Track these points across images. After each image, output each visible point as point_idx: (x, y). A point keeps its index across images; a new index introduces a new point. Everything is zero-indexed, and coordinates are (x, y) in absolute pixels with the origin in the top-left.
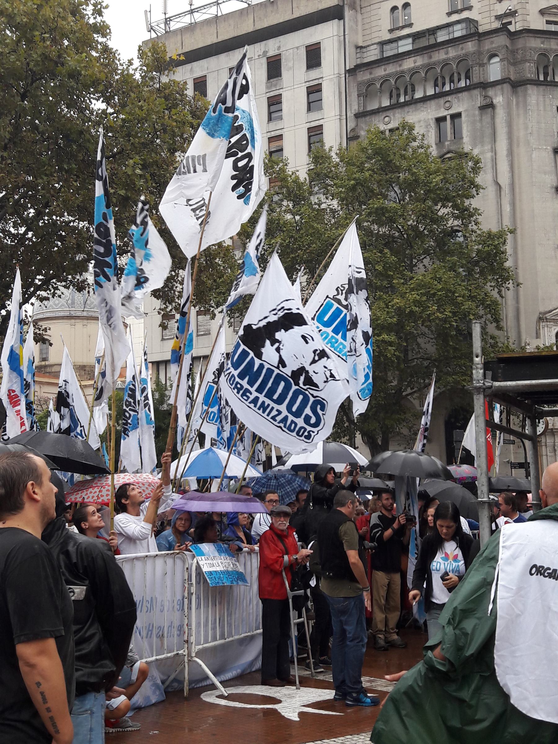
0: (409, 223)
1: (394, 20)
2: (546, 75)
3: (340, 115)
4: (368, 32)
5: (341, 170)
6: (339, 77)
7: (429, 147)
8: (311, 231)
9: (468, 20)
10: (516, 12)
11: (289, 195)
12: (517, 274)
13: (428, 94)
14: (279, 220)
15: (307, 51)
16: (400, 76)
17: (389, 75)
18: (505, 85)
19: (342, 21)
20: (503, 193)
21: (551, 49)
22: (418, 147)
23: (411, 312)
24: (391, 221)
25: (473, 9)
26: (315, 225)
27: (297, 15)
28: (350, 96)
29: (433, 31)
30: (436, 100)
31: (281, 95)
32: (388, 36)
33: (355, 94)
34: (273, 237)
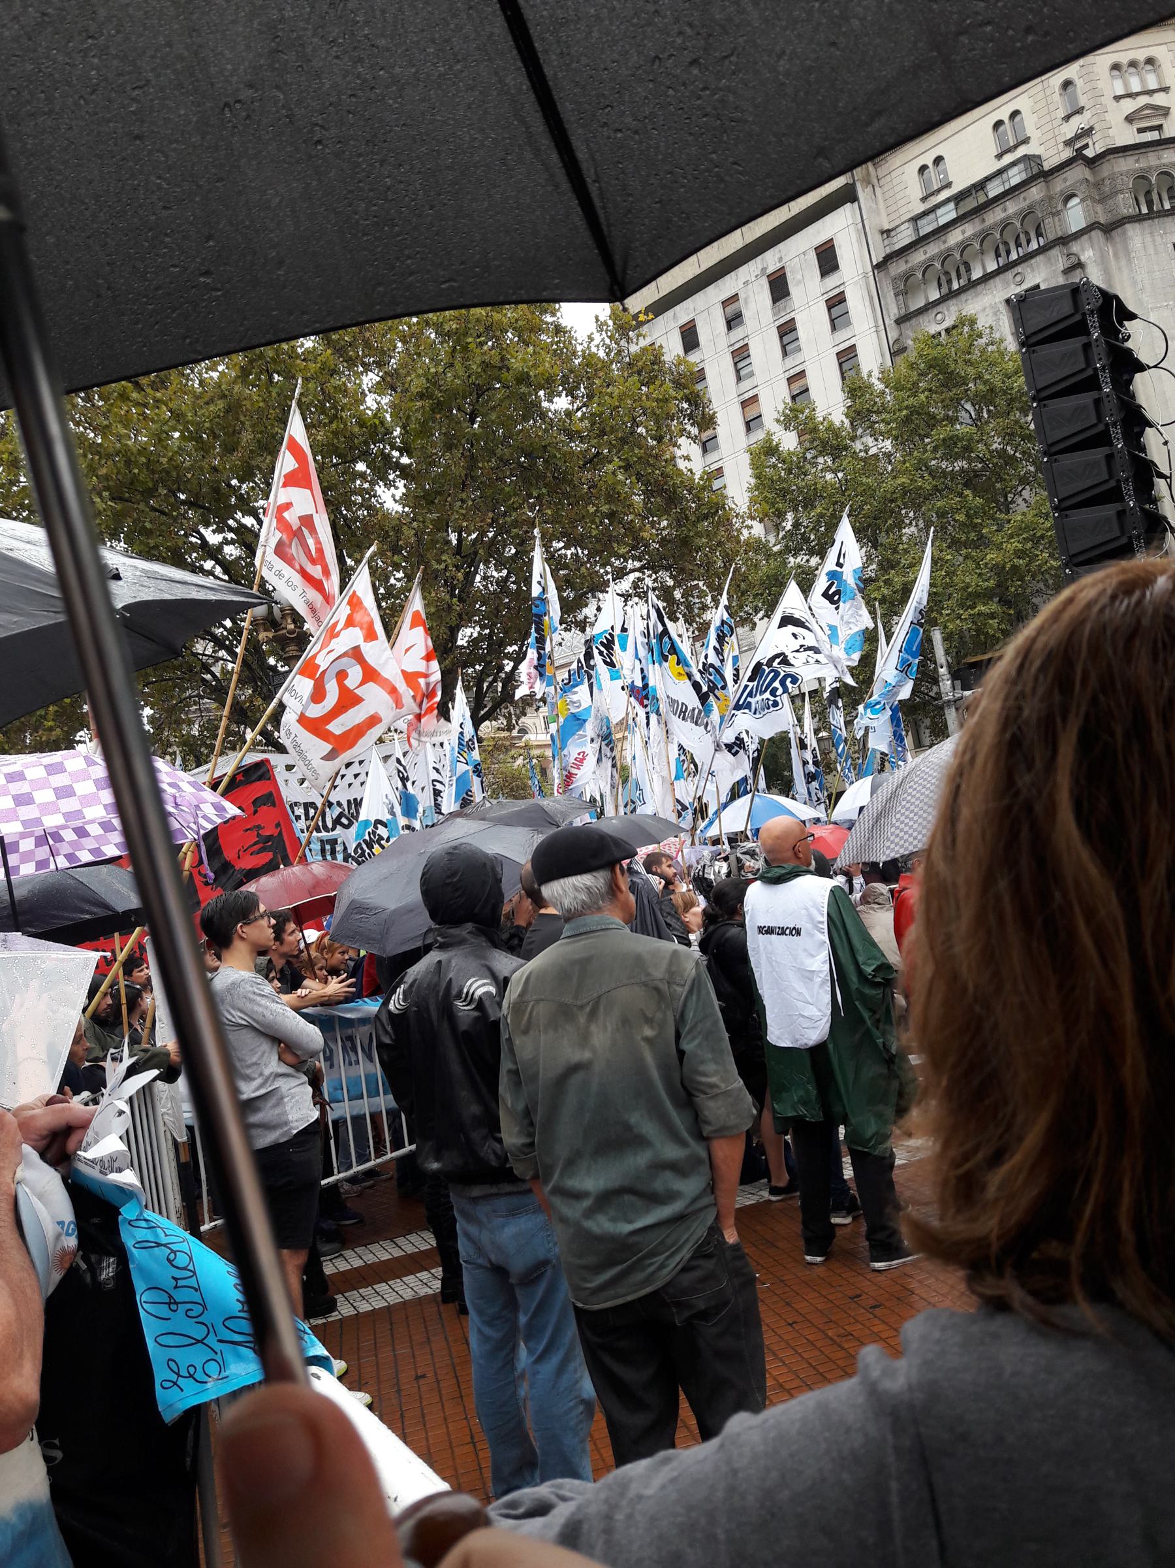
0: (995, 446)
1: (926, 184)
2: (1150, 204)
3: (877, 326)
4: (894, 208)
5: (889, 398)
6: (866, 277)
7: (1002, 341)
8: (860, 489)
9: (1026, 158)
10: (1091, 129)
11: (824, 447)
14: (816, 484)
15: (818, 255)
16: (946, 257)
17: (932, 258)
18: (1093, 233)
19: (856, 204)
22: (987, 345)
23: (1014, 567)
24: (968, 449)
25: (1032, 141)
26: (864, 480)
28: (885, 298)
29: (980, 186)
30: (1002, 276)
32: (922, 208)
33: (891, 295)
34: (813, 507)
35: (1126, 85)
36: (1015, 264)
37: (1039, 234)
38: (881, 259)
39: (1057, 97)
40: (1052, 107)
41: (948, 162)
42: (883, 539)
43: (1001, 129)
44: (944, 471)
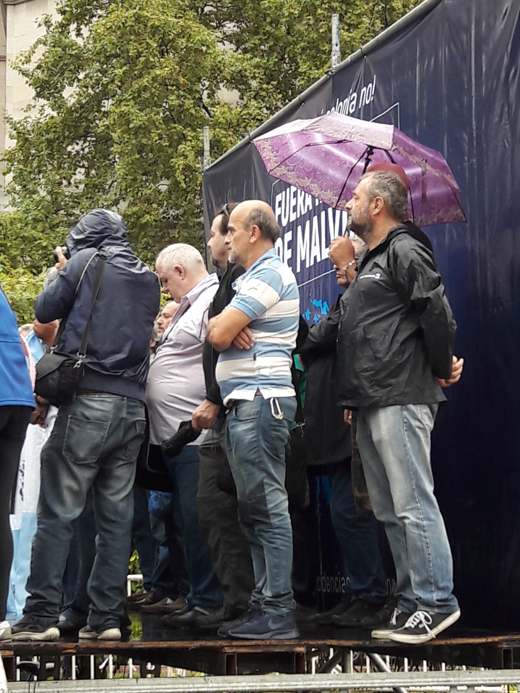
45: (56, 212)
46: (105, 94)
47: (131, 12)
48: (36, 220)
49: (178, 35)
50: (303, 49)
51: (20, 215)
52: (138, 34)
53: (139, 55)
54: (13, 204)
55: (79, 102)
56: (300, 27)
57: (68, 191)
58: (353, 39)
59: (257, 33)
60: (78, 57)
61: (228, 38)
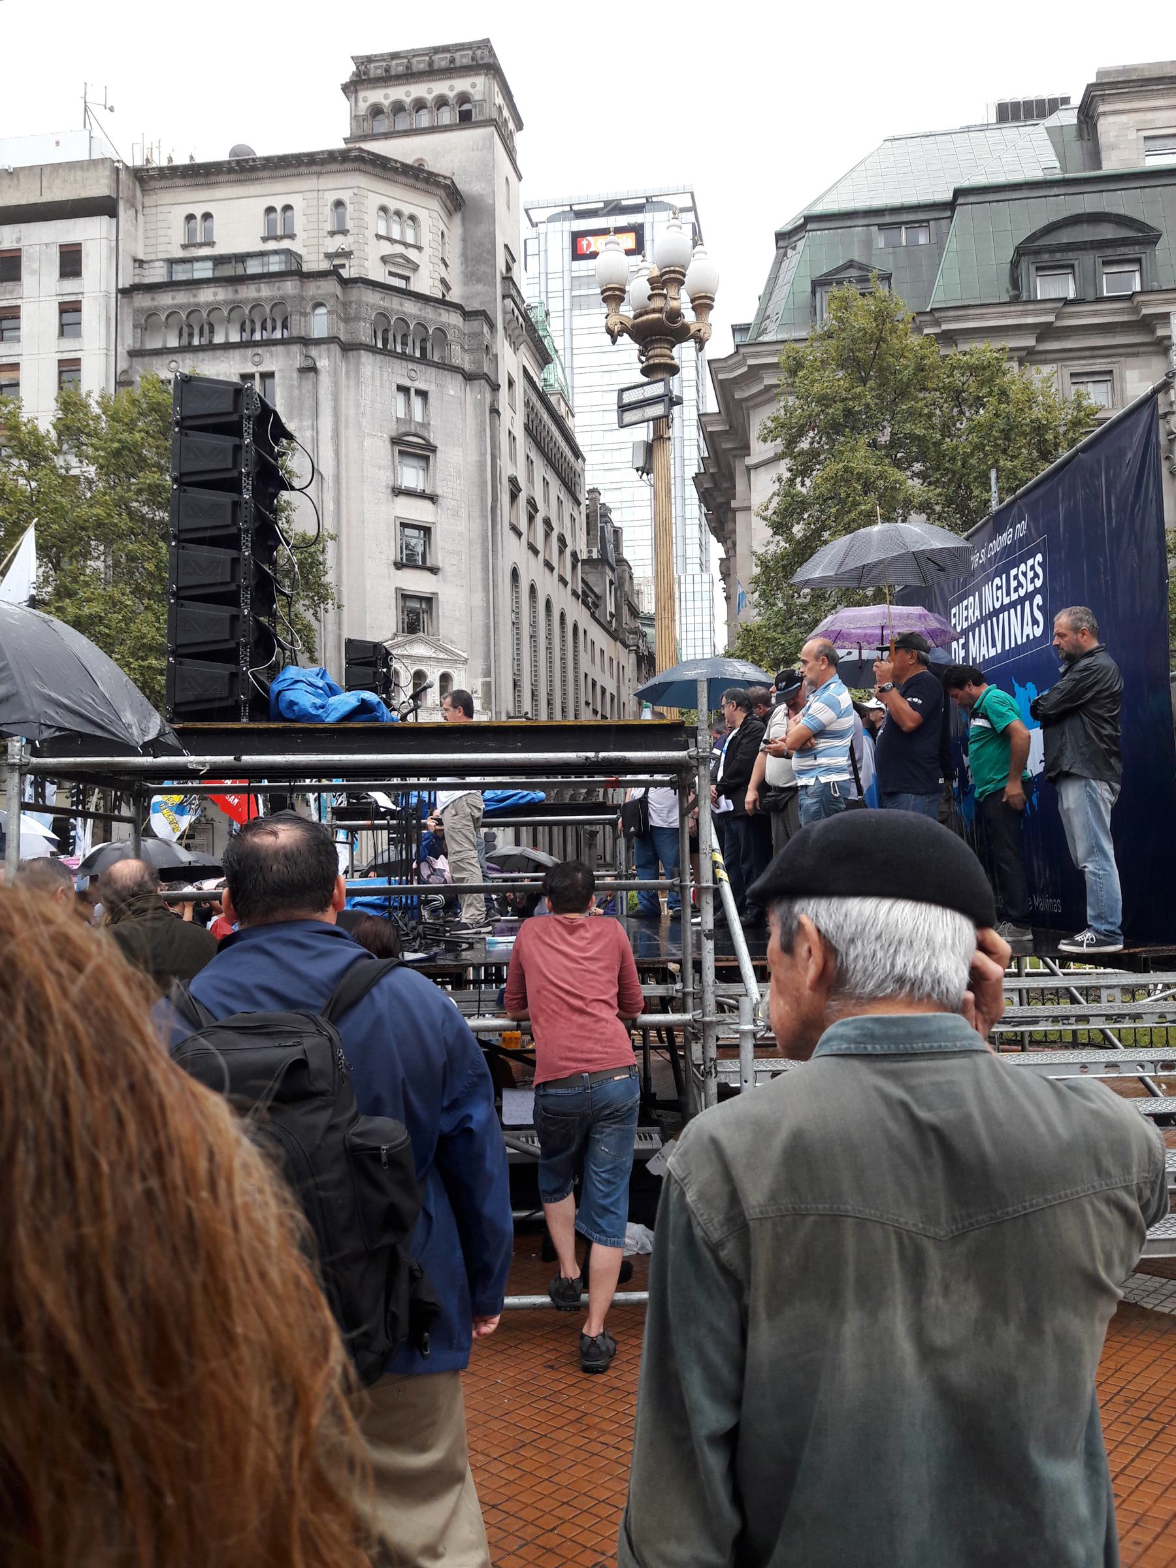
1: (191, 233)
2: (385, 341)
4: (153, 241)
6: (107, 296)
8: (51, 506)
9: (288, 252)
10: (351, 253)
11: (23, 450)
12: (339, 592)
13: (232, 340)
16: (194, 311)
17: (180, 306)
18: (332, 346)
19: (114, 220)
20: (325, 485)
21: (392, 310)
25: (298, 240)
26: (58, 498)
27: (48, 197)
28: (122, 325)
29: (242, 258)
30: (242, 351)
31: (19, 307)
32: (180, 254)
35: (388, 228)
36: (256, 344)
37: (285, 326)
38: (127, 286)
39: (327, 210)
40: (322, 218)
41: (217, 223)
42: (65, 564)
43: (272, 215)
44: (143, 516)
45: (791, 618)
46: (824, 528)
47: (841, 465)
48: (776, 625)
49: (878, 478)
50: (975, 478)
51: (764, 622)
52: (846, 481)
53: (848, 496)
54: (759, 615)
55: (804, 535)
56: (973, 461)
57: (798, 602)
58: (1015, 467)
59: (938, 469)
60: (802, 502)
61: (915, 475)
